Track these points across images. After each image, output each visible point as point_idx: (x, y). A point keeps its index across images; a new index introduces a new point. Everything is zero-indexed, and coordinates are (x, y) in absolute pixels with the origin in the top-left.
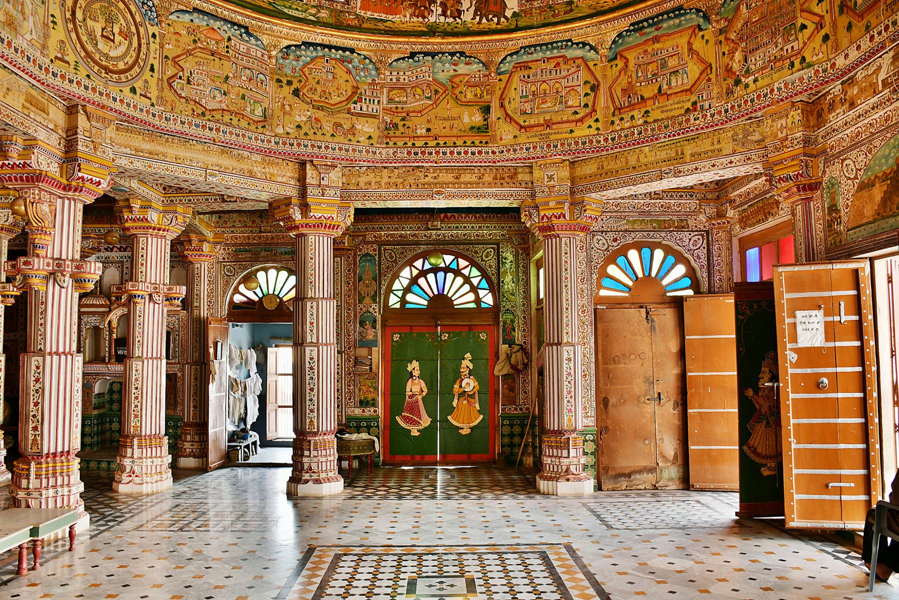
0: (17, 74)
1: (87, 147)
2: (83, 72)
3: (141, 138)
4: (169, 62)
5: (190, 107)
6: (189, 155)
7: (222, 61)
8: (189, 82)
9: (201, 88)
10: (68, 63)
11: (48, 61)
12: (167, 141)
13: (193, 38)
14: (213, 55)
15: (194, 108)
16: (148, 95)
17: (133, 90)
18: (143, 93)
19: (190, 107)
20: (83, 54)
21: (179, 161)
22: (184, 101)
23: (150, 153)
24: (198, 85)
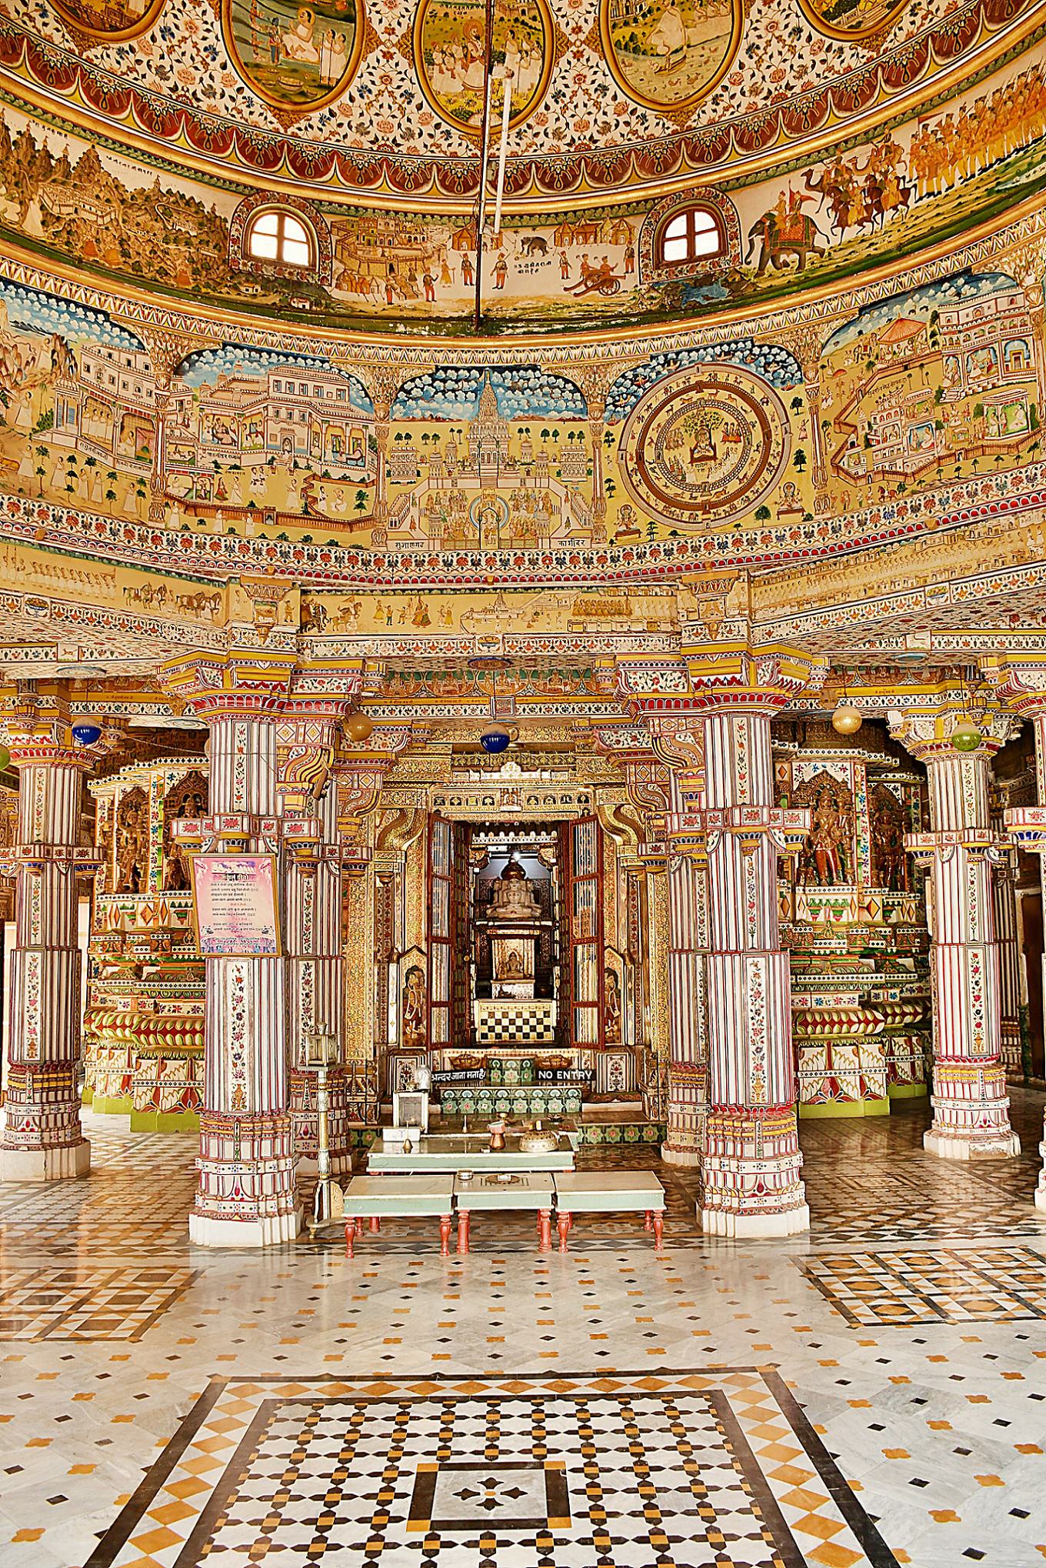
0: (552, 588)
1: (697, 635)
2: (663, 531)
4: (831, 429)
5: (875, 487)
6: (887, 574)
7: (925, 369)
8: (868, 445)
9: (893, 441)
10: (638, 532)
11: (606, 545)
13: (866, 360)
14: (906, 368)
15: (884, 484)
16: (796, 506)
17: (763, 513)
18: (785, 507)
19: (875, 487)
20: (661, 506)
21: (870, 593)
22: (863, 481)
24: (885, 440)
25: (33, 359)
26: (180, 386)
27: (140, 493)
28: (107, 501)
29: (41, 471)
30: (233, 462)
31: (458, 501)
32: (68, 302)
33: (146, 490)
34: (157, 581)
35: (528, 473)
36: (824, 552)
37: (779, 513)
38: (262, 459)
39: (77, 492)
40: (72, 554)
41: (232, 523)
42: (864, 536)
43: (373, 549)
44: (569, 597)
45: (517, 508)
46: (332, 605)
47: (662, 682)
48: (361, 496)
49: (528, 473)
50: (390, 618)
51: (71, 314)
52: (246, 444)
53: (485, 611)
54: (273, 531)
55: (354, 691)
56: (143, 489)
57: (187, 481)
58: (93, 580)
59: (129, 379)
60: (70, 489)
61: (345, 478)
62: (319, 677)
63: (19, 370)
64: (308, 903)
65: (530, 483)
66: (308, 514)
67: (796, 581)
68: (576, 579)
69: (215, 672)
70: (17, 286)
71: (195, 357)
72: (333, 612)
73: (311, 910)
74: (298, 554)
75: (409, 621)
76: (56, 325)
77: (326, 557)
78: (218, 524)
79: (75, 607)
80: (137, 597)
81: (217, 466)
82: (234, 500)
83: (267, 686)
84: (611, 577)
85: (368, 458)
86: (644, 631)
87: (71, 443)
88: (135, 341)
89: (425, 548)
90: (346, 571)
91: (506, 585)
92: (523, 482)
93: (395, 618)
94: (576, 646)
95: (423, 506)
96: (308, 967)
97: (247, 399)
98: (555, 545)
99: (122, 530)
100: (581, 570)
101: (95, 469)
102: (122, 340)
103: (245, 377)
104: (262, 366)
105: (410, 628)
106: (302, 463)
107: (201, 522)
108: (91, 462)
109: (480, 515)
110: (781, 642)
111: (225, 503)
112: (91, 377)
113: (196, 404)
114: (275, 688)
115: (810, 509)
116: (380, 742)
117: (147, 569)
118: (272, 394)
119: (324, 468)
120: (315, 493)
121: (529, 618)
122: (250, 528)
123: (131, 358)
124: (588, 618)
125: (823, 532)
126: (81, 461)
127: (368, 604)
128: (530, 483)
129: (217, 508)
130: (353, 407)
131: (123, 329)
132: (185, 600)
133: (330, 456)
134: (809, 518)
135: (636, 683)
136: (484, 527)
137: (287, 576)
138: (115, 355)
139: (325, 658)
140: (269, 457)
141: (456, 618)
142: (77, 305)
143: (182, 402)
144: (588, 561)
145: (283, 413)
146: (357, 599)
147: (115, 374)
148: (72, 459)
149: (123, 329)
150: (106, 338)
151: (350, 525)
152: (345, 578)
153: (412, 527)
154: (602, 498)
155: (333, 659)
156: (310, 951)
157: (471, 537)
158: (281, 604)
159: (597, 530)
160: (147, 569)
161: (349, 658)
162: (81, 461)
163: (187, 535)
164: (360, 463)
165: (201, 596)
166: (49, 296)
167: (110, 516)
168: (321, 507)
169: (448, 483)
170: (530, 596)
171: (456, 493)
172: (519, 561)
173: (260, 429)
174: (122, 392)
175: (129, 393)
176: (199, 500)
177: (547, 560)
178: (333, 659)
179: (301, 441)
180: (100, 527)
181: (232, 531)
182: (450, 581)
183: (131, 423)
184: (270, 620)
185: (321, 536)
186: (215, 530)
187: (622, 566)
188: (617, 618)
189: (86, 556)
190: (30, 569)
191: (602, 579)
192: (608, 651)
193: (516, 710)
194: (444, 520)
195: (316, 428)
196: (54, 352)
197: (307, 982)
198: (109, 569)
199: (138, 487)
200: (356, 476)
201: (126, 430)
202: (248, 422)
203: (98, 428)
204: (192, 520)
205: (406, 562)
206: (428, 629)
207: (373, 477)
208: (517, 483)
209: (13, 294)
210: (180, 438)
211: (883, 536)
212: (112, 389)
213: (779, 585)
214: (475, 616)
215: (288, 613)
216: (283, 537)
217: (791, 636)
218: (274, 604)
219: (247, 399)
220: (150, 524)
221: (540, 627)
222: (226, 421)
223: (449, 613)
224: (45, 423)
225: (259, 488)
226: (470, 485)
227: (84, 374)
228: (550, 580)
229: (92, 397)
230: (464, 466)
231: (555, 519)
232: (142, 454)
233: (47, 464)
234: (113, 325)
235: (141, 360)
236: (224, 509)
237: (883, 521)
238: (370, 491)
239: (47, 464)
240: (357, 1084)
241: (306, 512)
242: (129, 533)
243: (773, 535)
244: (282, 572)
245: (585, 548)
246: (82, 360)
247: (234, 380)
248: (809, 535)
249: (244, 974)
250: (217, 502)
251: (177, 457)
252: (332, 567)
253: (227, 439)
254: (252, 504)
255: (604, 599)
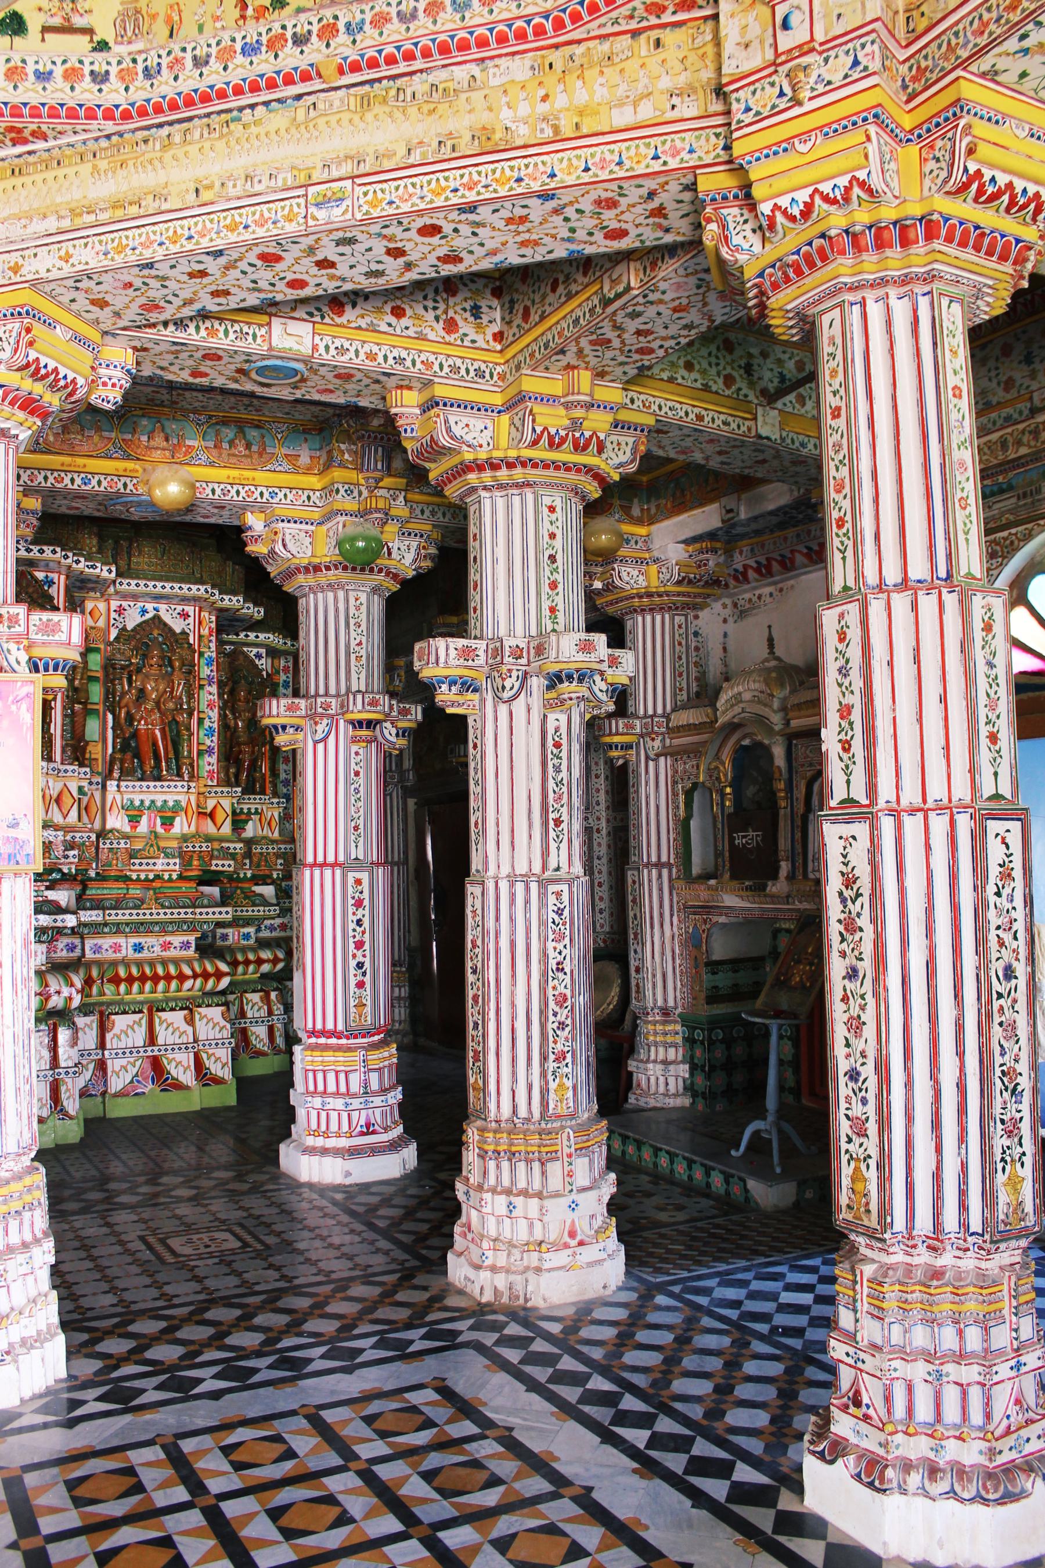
3: (86, 168)
6: (239, 163)
12: (168, 143)
16: (78, 21)
18: (57, 21)
21: (206, 196)
23: (117, 205)
36: (126, 116)
37: (46, 29)
42: (202, 87)
67: (70, 171)
110: (35, 284)
115: (105, 32)
125: (126, 77)
134: (102, 46)
211: (238, 91)
213: (39, 178)
217: (55, 274)
237: (240, 59)
243: (30, 69)
248: (100, 78)
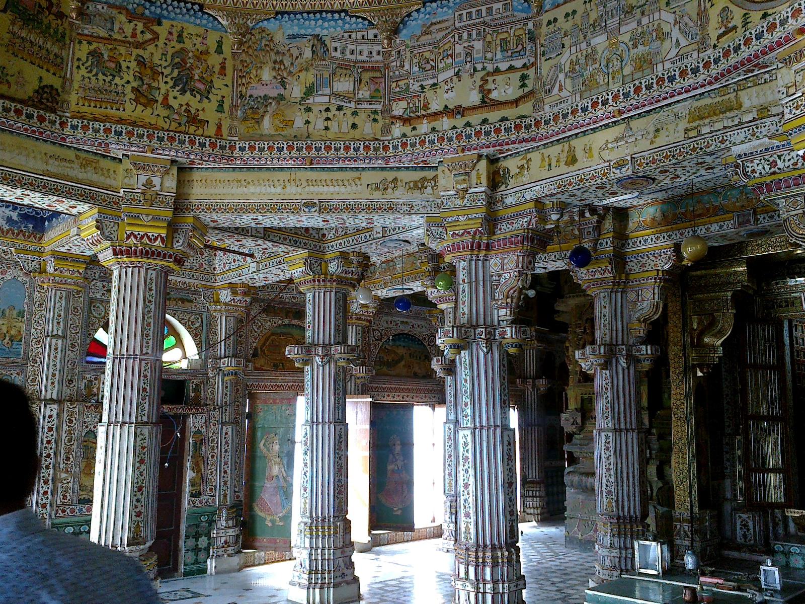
0: (670, 104)
10: (735, 27)
25: (300, 54)
26: (398, 41)
27: (375, 120)
28: (352, 131)
29: (308, 122)
30: (431, 82)
31: (591, 57)
32: (321, 12)
33: (379, 117)
34: (390, 176)
35: (643, 13)
38: (451, 73)
39: (332, 130)
40: (332, 169)
41: (433, 124)
43: (534, 115)
44: (683, 109)
45: (635, 46)
46: (512, 164)
47: (780, 164)
48: (524, 78)
49: (643, 13)
50: (550, 165)
51: (322, 19)
52: (441, 66)
53: (617, 140)
54: (460, 122)
55: (533, 225)
56: (377, 117)
57: (403, 104)
58: (346, 183)
59: (364, 48)
60: (327, 128)
61: (511, 68)
62: (510, 219)
63: (292, 64)
64: (606, 389)
65: (645, 21)
66: (487, 103)
68: (688, 91)
69: (441, 229)
70: (289, 13)
71: (407, 19)
72: (514, 170)
73: (608, 394)
74: (478, 134)
75: (562, 164)
76: (314, 29)
77: (498, 131)
78: (424, 127)
79: (335, 202)
80: (377, 188)
81: (422, 87)
82: (435, 107)
83: (469, 233)
84: (716, 79)
85: (529, 47)
86: (755, 120)
87: (326, 99)
88: (366, 22)
89: (570, 102)
90: (513, 137)
91: (631, 114)
92: (639, 22)
93: (554, 164)
94: (694, 150)
95: (567, 69)
96: (607, 437)
97: (440, 35)
98: (668, 65)
99: (362, 147)
100: (690, 81)
101: (342, 112)
102: (357, 24)
103: (439, 19)
104: (449, 8)
105: (564, 169)
106: (479, 67)
107: (414, 129)
108: (340, 108)
109: (608, 60)
111: (429, 111)
112: (338, 54)
113: (407, 50)
114: (475, 233)
116: (652, 264)
117: (382, 169)
118: (457, 25)
119: (495, 66)
120: (490, 86)
121: (651, 136)
122: (445, 124)
123: (365, 33)
124: (702, 122)
126: (333, 109)
127: (535, 156)
128: (645, 21)
129: (423, 117)
130: (516, 13)
131: (358, 17)
132: (412, 185)
133: (499, 56)
135: (754, 171)
136: (611, 71)
137: (473, 152)
138: (354, 36)
139: (511, 206)
140: (456, 69)
141: (595, 152)
142: (327, 12)
143: (399, 52)
144: (695, 71)
145: (465, 36)
146: (529, 156)
147: (353, 47)
148: (327, 110)
149: (358, 17)
150: (347, 26)
151: (516, 102)
152: (513, 143)
153: (560, 90)
154: (706, 10)
155: (516, 205)
156: (610, 425)
157: (601, 83)
158: (474, 173)
159: (702, 41)
160: (382, 169)
161: (527, 202)
162: (333, 109)
163: (404, 140)
164: (522, 53)
165: (424, 179)
166: (309, 13)
167: (354, 140)
168: (494, 95)
169: (584, 46)
170: (654, 117)
171: (590, 50)
172: (638, 90)
173: (449, 53)
174: (359, 58)
175: (364, 57)
176: (412, 114)
177: (660, 80)
178: (516, 205)
179: (478, 52)
180: (347, 148)
181: (434, 129)
182: (589, 124)
183: (366, 76)
184: (464, 186)
185: (494, 116)
186: (423, 132)
187: (723, 65)
188: (728, 114)
189: (341, 169)
190: (305, 184)
191: (710, 83)
192: (723, 146)
193: (757, 220)
194: (582, 75)
195: (489, 38)
196: (313, 46)
197: (607, 449)
198: (356, 174)
199: (373, 116)
200: (518, 63)
201: (363, 82)
202: (441, 50)
203: (343, 85)
204: (407, 129)
205: (556, 118)
206: (577, 166)
207: (532, 60)
208: (634, 25)
209: (287, 19)
210: (400, 76)
212: (353, 57)
214: (610, 146)
215: (478, 178)
216: (468, 124)
218: (467, 174)
219: (440, 35)
220: (382, 138)
221: (662, 140)
222: (427, 55)
223: (590, 149)
224: (309, 91)
225: (450, 94)
226: (600, 41)
227: (334, 54)
228: (666, 98)
229: (340, 66)
230: (594, 26)
231: (667, 44)
232: (375, 94)
233: (311, 117)
234: (351, 17)
235: (371, 33)
236: (428, 116)
238: (531, 72)
239: (311, 117)
240: (685, 532)
241: (483, 101)
242: (367, 148)
244: (469, 150)
245: (694, 59)
246: (331, 45)
247: (432, 24)
249: (469, 439)
250: (423, 112)
251: (398, 89)
252: (503, 136)
253: (428, 67)
254: (446, 107)
255: (715, 100)
